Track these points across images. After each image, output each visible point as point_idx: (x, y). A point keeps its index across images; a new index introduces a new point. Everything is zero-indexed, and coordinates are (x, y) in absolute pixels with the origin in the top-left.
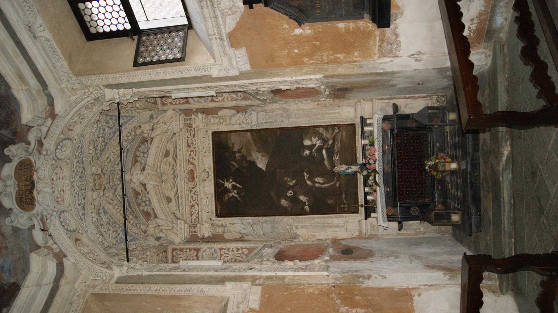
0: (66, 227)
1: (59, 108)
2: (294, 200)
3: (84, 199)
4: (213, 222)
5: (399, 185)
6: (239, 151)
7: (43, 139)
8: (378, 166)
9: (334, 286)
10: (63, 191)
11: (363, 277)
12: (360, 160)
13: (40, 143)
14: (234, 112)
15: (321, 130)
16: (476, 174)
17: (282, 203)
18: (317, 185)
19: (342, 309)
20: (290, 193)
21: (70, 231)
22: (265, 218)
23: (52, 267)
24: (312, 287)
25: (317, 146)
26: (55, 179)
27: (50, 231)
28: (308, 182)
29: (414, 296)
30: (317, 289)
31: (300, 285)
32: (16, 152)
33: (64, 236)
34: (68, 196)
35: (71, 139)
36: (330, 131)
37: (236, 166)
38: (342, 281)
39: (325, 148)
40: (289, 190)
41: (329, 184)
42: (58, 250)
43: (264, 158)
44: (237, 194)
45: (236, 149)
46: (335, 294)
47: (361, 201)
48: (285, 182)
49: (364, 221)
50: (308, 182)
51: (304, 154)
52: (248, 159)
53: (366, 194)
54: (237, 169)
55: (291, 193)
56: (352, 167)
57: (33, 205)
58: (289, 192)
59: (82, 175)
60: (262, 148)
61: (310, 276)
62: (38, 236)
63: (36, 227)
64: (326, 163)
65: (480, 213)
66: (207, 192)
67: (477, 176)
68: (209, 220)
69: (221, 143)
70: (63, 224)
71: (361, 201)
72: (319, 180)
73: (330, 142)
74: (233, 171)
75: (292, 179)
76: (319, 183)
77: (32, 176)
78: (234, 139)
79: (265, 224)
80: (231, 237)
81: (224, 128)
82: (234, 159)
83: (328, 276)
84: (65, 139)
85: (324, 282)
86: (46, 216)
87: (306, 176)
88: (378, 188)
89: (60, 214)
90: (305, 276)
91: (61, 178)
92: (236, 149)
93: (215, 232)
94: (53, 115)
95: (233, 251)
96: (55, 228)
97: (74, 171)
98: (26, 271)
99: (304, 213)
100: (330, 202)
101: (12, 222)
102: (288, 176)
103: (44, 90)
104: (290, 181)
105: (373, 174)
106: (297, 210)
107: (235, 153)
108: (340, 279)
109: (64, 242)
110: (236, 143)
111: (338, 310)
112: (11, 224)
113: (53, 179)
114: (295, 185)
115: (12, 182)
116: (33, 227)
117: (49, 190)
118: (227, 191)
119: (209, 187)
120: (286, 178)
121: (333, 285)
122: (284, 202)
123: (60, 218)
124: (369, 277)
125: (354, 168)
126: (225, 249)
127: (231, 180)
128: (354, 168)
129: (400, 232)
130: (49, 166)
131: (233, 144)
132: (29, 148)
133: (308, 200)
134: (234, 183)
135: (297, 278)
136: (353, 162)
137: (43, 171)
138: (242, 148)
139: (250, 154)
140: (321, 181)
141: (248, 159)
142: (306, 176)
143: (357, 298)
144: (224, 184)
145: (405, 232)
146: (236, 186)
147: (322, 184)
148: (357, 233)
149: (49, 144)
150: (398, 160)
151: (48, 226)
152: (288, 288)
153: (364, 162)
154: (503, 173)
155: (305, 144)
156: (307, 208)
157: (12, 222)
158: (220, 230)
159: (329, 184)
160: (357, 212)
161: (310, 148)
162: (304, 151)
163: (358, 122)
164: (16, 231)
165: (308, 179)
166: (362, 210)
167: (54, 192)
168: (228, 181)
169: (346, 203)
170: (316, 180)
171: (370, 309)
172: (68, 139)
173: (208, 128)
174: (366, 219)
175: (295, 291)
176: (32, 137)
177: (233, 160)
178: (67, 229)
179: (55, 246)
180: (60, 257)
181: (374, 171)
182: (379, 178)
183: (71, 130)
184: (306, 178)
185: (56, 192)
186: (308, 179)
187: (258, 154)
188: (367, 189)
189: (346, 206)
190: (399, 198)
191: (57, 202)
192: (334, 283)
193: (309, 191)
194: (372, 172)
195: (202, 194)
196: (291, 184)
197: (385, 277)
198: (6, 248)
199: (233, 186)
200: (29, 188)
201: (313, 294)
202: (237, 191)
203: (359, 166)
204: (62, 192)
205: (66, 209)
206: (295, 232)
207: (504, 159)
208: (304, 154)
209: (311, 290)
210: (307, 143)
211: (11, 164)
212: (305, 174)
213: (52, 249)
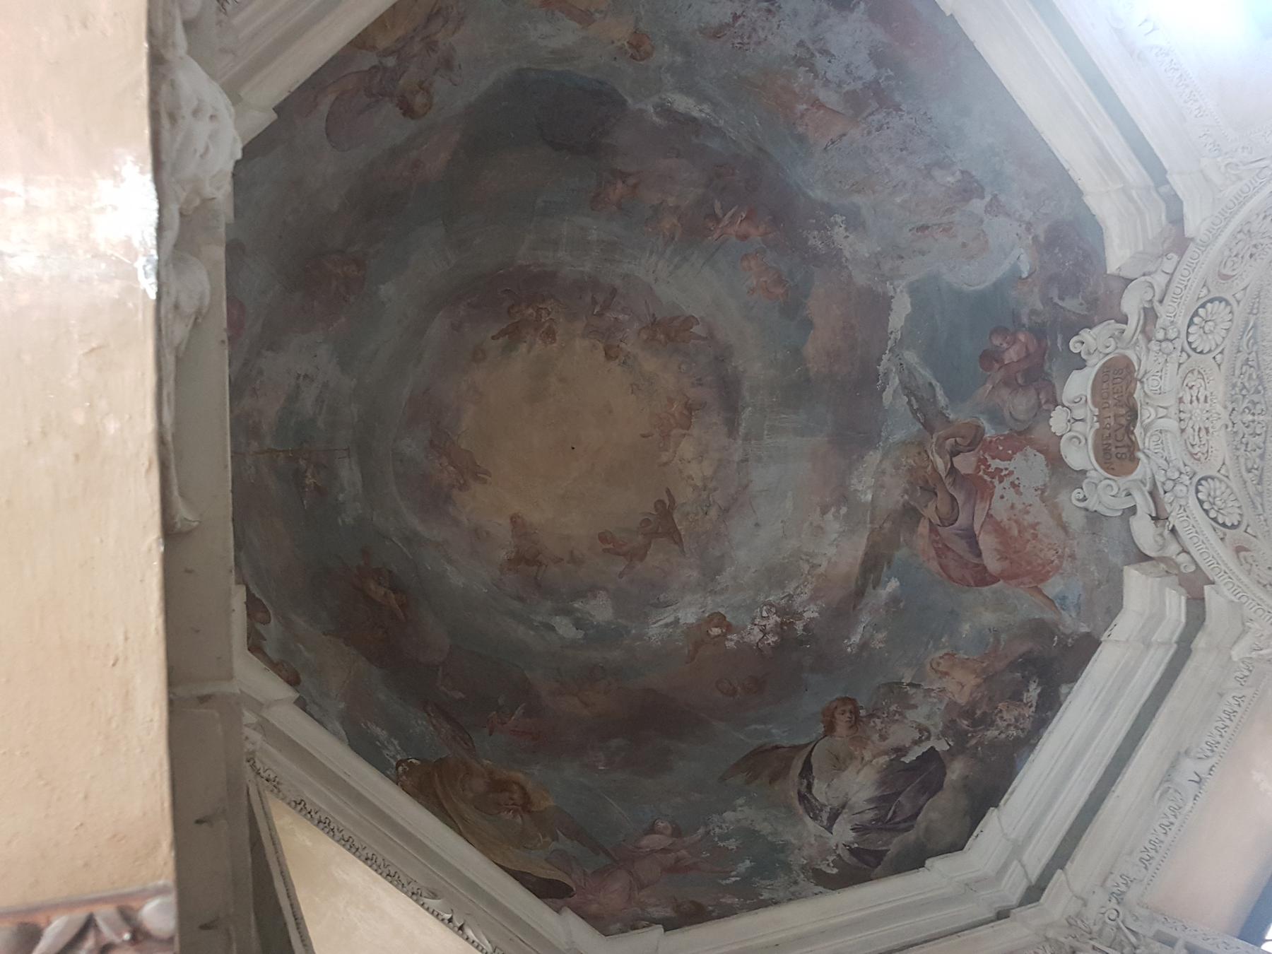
0: (1213, 514)
1: (1194, 223)
3: (1262, 457)
7: (1156, 304)
10: (1207, 429)
13: (1150, 315)
21: (1224, 525)
23: (1176, 606)
26: (1187, 399)
27: (1173, 521)
32: (1094, 343)
33: (1209, 533)
34: (1219, 446)
35: (1228, 303)
42: (1192, 568)
57: (1135, 461)
59: (1256, 398)
62: (1144, 533)
63: (1139, 512)
70: (1206, 506)
77: (1131, 395)
84: (1211, 301)
86: (1164, 484)
89: (1199, 483)
91: (1202, 399)
94: (1181, 244)
96: (1188, 517)
97: (1234, 386)
98: (1114, 607)
101: (1085, 499)
103: (1157, 188)
109: (1208, 549)
112: (1082, 505)
113: (1181, 400)
115: (1087, 411)
116: (1133, 510)
117: (1172, 424)
123: (1197, 491)
130: (1172, 367)
132: (1123, 332)
137: (1159, 381)
149: (1173, 314)
151: (1168, 509)
157: (1085, 499)
164: (1094, 518)
167: (1183, 431)
172: (1221, 300)
176: (1131, 304)
178: (1215, 520)
179: (1183, 558)
180: (1195, 591)
183: (1226, 277)
185: (1189, 430)
191: (1192, 455)
198: (1072, 557)
200: (1123, 421)
204: (1203, 433)
205: (1213, 473)
211: (1086, 370)
213: (1177, 566)
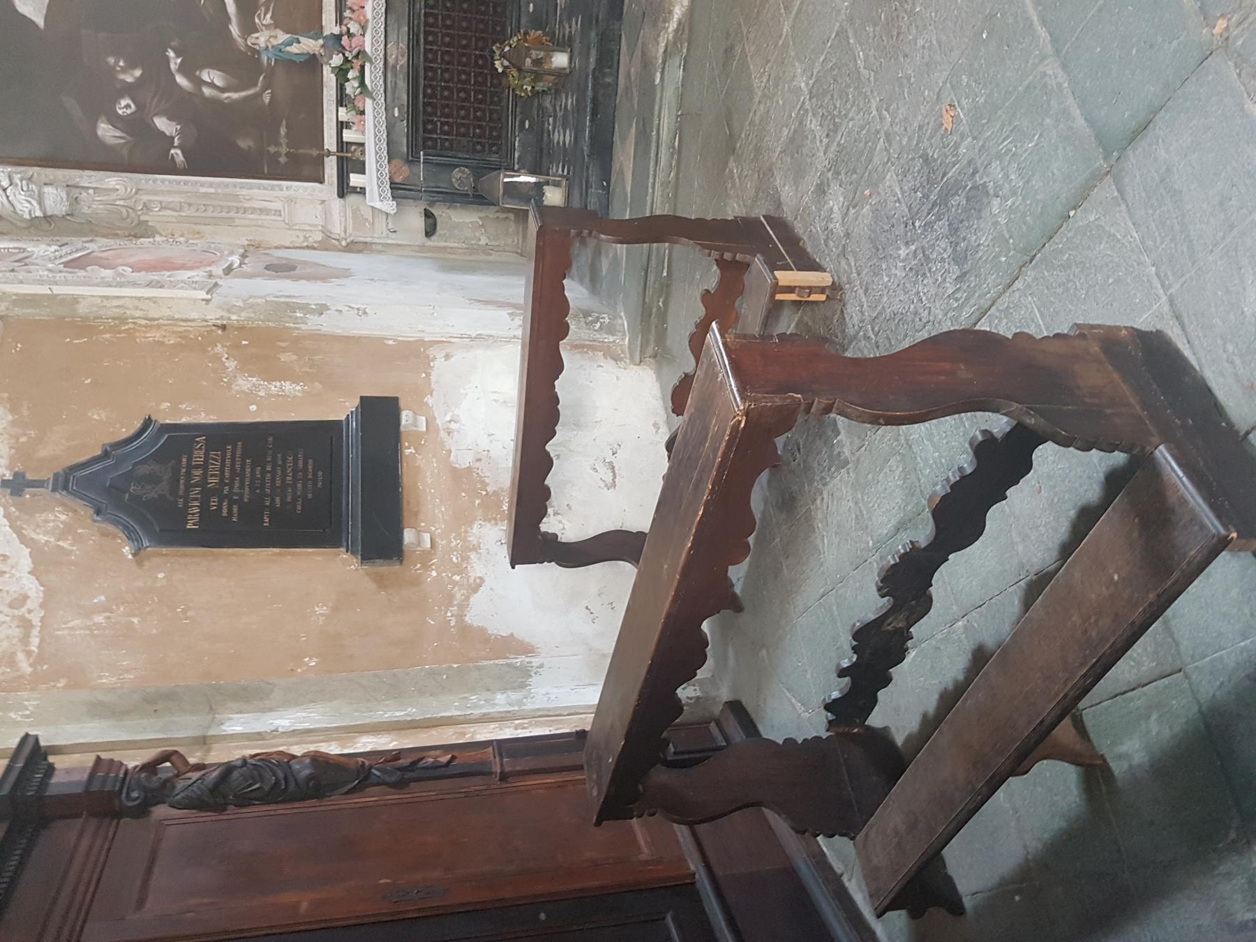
5: (425, 104)
8: (371, 43)
9: (224, 327)
11: (305, 308)
16: (608, 80)
17: (100, 133)
18: (207, 91)
19: (240, 382)
20: (125, 106)
24: (159, 326)
28: (181, 80)
29: (435, 358)
30: (174, 332)
31: (122, 320)
38: (244, 315)
40: (122, 97)
41: (243, 94)
46: (223, 346)
48: (112, 71)
49: (336, 203)
50: (181, 80)
53: (341, 126)
55: (128, 106)
56: (301, 39)
58: (123, 102)
61: (154, 300)
64: (234, 29)
65: (608, 184)
67: (609, 84)
72: (211, 76)
75: (131, 66)
76: (212, 85)
79: (47, 189)
83: (208, 301)
85: (194, 315)
87: (175, 62)
88: (368, 102)
90: (139, 299)
99: (170, 168)
100: (244, 144)
104: (124, 70)
105: (357, 64)
108: (242, 309)
111: (229, 384)
121: (219, 322)
122: (106, 131)
124: (322, 309)
128: (309, 45)
129: (429, 243)
133: (181, 133)
135: (115, 303)
140: (218, 82)
142: (175, 62)
143: (284, 357)
145: (443, 244)
148: (318, 237)
150: (426, 34)
152: (87, 327)
153: (336, 30)
154: (664, 62)
156: (177, 153)
159: (243, 94)
160: (321, 181)
165: (182, 69)
166: (331, 167)
169: (283, 141)
170: (205, 77)
171: (318, 386)
174: (341, 194)
175: (107, 336)
181: (361, 54)
182: (373, 76)
184: (173, 66)
186: (182, 69)
188: (344, 114)
189: (284, 150)
190: (425, 140)
192: (222, 318)
193: (181, 106)
194: (357, 57)
196: (129, 79)
197: (365, 313)
201: (163, 343)
203: (321, 41)
206: (142, 218)
207: (673, 25)
209: (154, 335)
212: (171, 54)
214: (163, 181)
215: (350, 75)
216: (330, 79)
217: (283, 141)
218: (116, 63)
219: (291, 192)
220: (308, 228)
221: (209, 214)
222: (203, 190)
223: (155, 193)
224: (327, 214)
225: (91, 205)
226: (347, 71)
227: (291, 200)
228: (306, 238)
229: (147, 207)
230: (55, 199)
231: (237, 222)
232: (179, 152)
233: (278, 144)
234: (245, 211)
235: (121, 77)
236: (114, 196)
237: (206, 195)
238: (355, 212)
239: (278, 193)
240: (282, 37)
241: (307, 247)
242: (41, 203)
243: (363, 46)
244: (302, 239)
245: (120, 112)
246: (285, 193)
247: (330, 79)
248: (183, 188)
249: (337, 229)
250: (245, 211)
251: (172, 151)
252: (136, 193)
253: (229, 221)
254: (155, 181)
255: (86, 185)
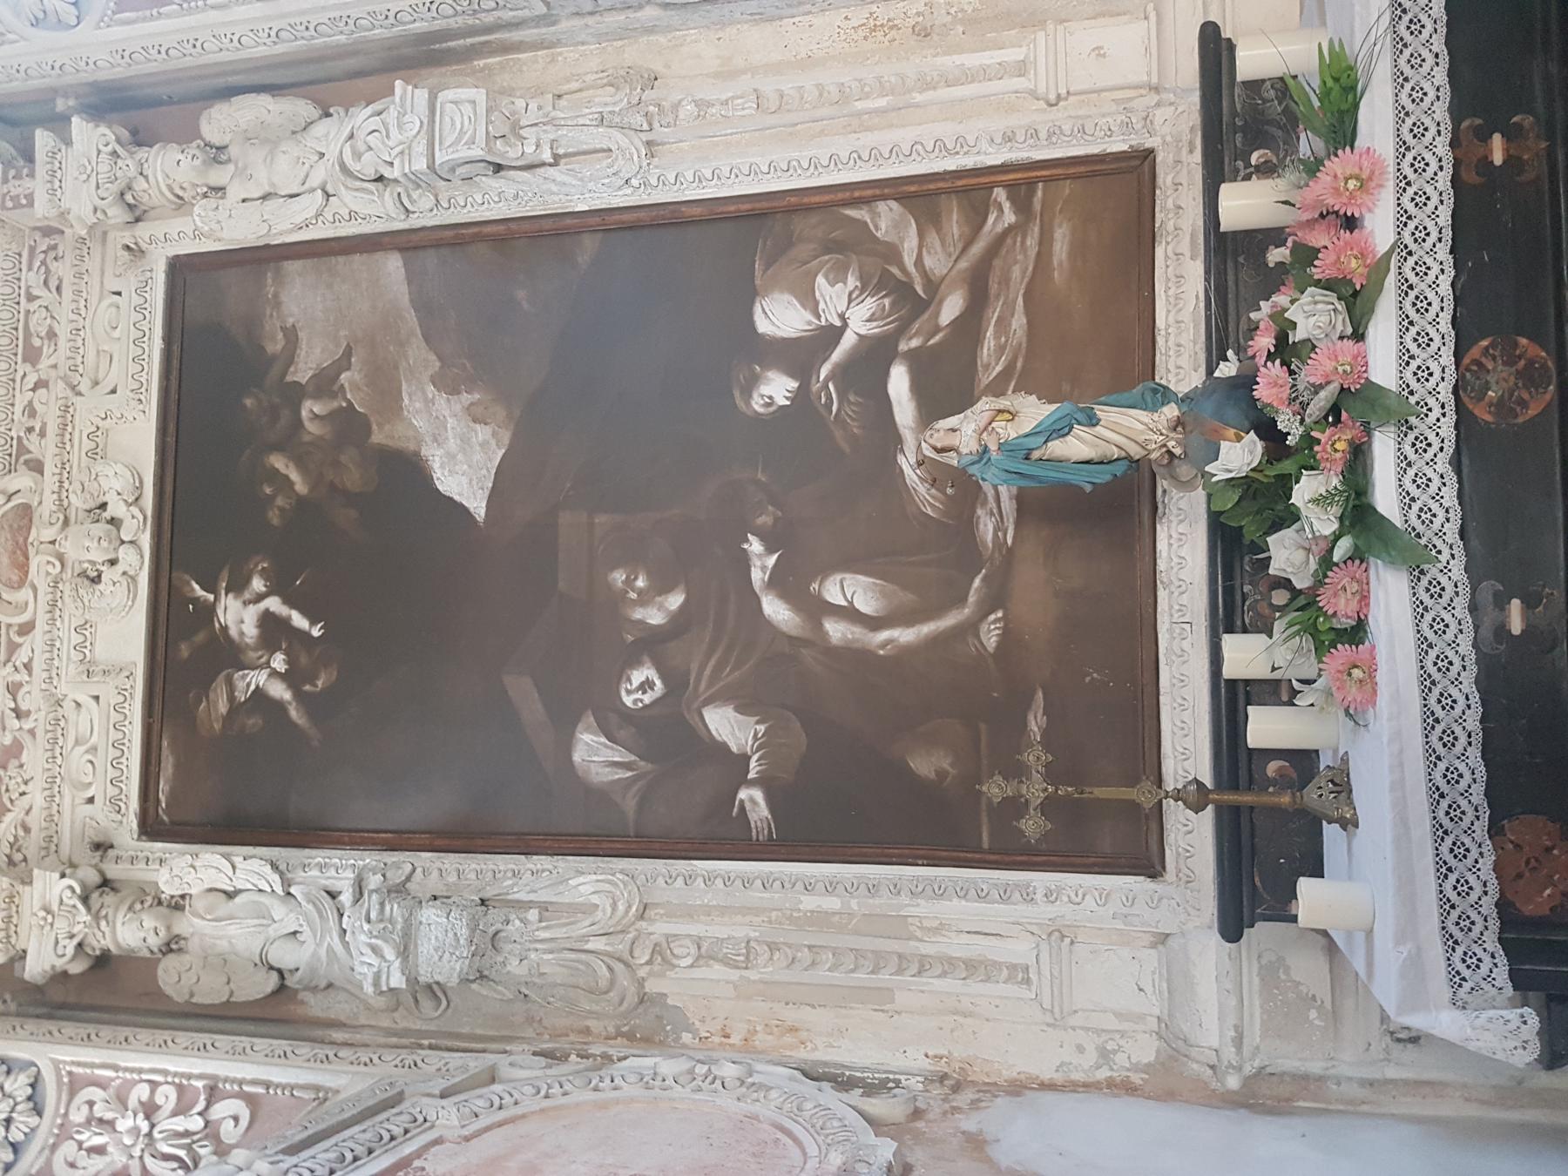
2: (668, 737)
4: (113, 871)
6: (325, 383)
12: (1181, 359)
14: (303, 108)
15: (886, 219)
17: (577, 757)
18: (836, 630)
20: (641, 686)
22: (450, 861)
25: (848, 340)
28: (776, 610)
36: (955, 225)
37: (301, 487)
39: (913, 358)
40: (636, 663)
43: (482, 433)
44: (289, 678)
45: (302, 372)
47: (1187, 749)
48: (617, 600)
50: (776, 610)
51: (757, 405)
52: (377, 437)
53: (1232, 700)
54: (301, 500)
55: (646, 685)
56: (1106, 414)
58: (638, 677)
60: (471, 363)
66: (102, 652)
68: (87, 857)
69: (215, 342)
71: (1187, 749)
72: (852, 590)
73: (951, 308)
74: (274, 518)
75: (662, 587)
76: (849, 613)
78: (301, 301)
80: (211, 992)
81: (235, 227)
82: (291, 441)
87: (761, 561)
92: (302, 372)
93: (102, 940)
95: (150, 1110)
99: (734, 842)
100: (926, 764)
102: (632, 559)
104: (644, 599)
105: (1335, 443)
106: (682, 818)
107: (296, 394)
110: (310, 322)
114: (680, 624)
118: (227, 654)
119: (124, 631)
120: (619, 577)
122: (595, 753)
125: (1127, 429)
126: (101, 1084)
127: (258, 584)
128: (1127, 429)
131: (291, 335)
133: (766, 744)
134: (274, 604)
136: (1133, 373)
138: (344, 363)
139: (389, 400)
140: (866, 604)
141: (377, 437)
142: (761, 561)
144: (211, 610)
146: (285, 623)
147: (874, 623)
148: (1143, 1050)
155: (763, 326)
158: (131, 932)
161: (800, 355)
162: (753, 382)
163: (1175, 131)
165: (777, 582)
168: (238, 586)
170: (833, 592)
173: (143, 231)
177: (278, 447)
182: (1410, 477)
184: (757, 576)
186: (777, 582)
187: (441, 400)
188: (1246, 656)
195: (70, 668)
196: (654, 617)
199: (269, 622)
202: (290, 662)
203: (1171, 411)
208: (757, 405)
210: (779, 317)
212: (755, 546)
214: (708, 880)
215: (1304, 491)
216: (1182, 551)
217: (1034, 757)
218: (629, 582)
219: (1061, 909)
220: (1112, 1023)
221: (822, 974)
222: (809, 903)
223: (690, 913)
224: (1176, 983)
225: (532, 952)
226: (1285, 484)
227: (1059, 934)
228: (1105, 1055)
229: (662, 954)
230: (441, 943)
231: (901, 998)
232: (758, 795)
233: (1017, 772)
234: (924, 966)
235: (638, 614)
236: (582, 928)
237: (820, 920)
238: (1271, 974)
239: (1021, 910)
240: (1033, 412)
241: (1111, 1084)
242: (405, 952)
243: (1362, 362)
244: (1091, 1057)
245: (628, 700)
246: (1043, 911)
247: (1182, 551)
248: (757, 895)
249: (1209, 1032)
250: (924, 966)
251: (743, 794)
252: (641, 917)
253: (880, 997)
254: (689, 879)
255: (522, 896)
